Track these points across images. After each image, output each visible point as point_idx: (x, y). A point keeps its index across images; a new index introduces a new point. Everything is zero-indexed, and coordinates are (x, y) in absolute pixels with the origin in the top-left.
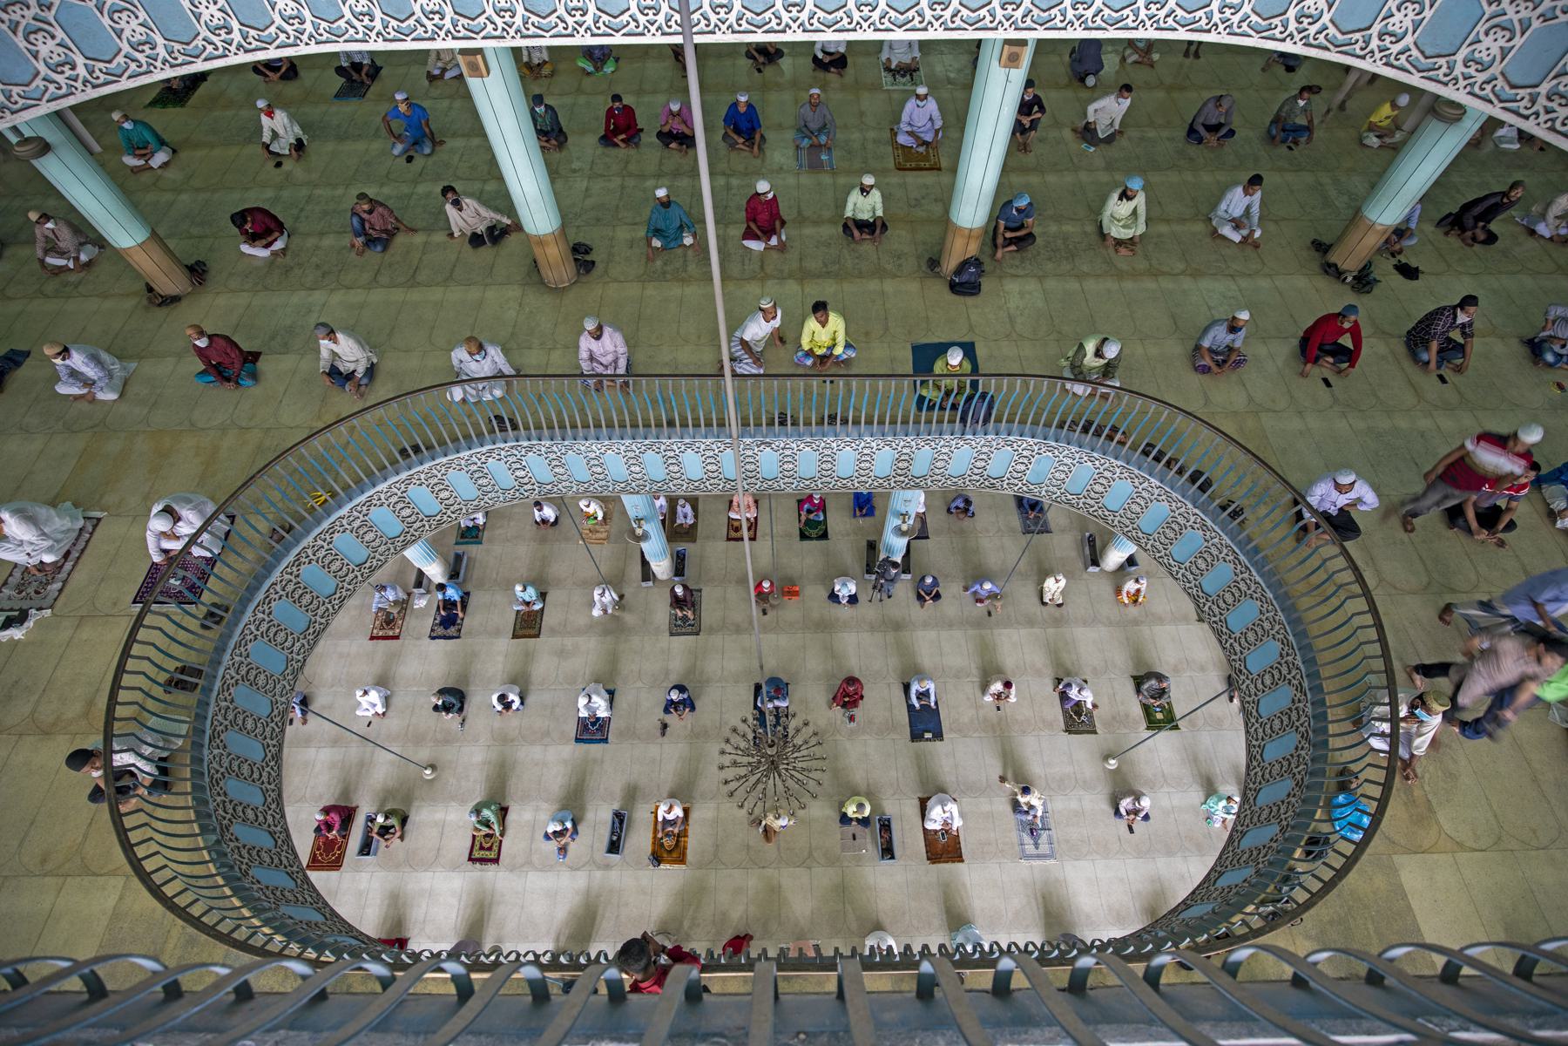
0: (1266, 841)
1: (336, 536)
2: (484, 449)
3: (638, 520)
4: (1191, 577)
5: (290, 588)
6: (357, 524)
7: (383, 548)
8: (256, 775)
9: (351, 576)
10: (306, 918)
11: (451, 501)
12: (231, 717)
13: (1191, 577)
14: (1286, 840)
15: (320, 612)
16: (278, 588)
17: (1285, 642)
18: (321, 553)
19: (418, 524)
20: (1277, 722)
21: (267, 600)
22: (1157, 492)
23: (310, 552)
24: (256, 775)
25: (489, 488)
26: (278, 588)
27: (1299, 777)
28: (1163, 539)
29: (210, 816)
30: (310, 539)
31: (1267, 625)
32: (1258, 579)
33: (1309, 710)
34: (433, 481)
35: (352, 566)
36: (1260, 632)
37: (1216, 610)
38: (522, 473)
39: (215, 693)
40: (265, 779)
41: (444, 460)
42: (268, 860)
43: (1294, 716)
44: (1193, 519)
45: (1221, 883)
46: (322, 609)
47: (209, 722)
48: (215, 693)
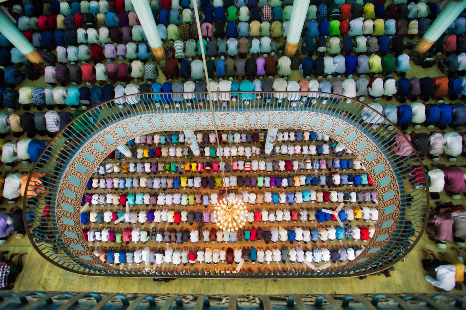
0: (384, 239)
1: (94, 144)
4: (362, 156)
5: (80, 160)
6: (100, 140)
7: (109, 147)
9: (100, 156)
10: (87, 259)
12: (63, 199)
13: (362, 156)
16: (77, 160)
17: (393, 177)
18: (90, 149)
19: (120, 140)
21: (73, 163)
23: (86, 149)
25: (141, 129)
26: (77, 160)
27: (395, 219)
28: (354, 144)
29: (57, 229)
31: (387, 172)
33: (400, 199)
34: (124, 126)
35: (100, 153)
37: (370, 167)
38: (151, 124)
39: (58, 192)
40: (75, 217)
42: (76, 242)
43: (394, 200)
44: (364, 138)
45: (370, 252)
46: (91, 166)
47: (56, 201)
48: (58, 192)
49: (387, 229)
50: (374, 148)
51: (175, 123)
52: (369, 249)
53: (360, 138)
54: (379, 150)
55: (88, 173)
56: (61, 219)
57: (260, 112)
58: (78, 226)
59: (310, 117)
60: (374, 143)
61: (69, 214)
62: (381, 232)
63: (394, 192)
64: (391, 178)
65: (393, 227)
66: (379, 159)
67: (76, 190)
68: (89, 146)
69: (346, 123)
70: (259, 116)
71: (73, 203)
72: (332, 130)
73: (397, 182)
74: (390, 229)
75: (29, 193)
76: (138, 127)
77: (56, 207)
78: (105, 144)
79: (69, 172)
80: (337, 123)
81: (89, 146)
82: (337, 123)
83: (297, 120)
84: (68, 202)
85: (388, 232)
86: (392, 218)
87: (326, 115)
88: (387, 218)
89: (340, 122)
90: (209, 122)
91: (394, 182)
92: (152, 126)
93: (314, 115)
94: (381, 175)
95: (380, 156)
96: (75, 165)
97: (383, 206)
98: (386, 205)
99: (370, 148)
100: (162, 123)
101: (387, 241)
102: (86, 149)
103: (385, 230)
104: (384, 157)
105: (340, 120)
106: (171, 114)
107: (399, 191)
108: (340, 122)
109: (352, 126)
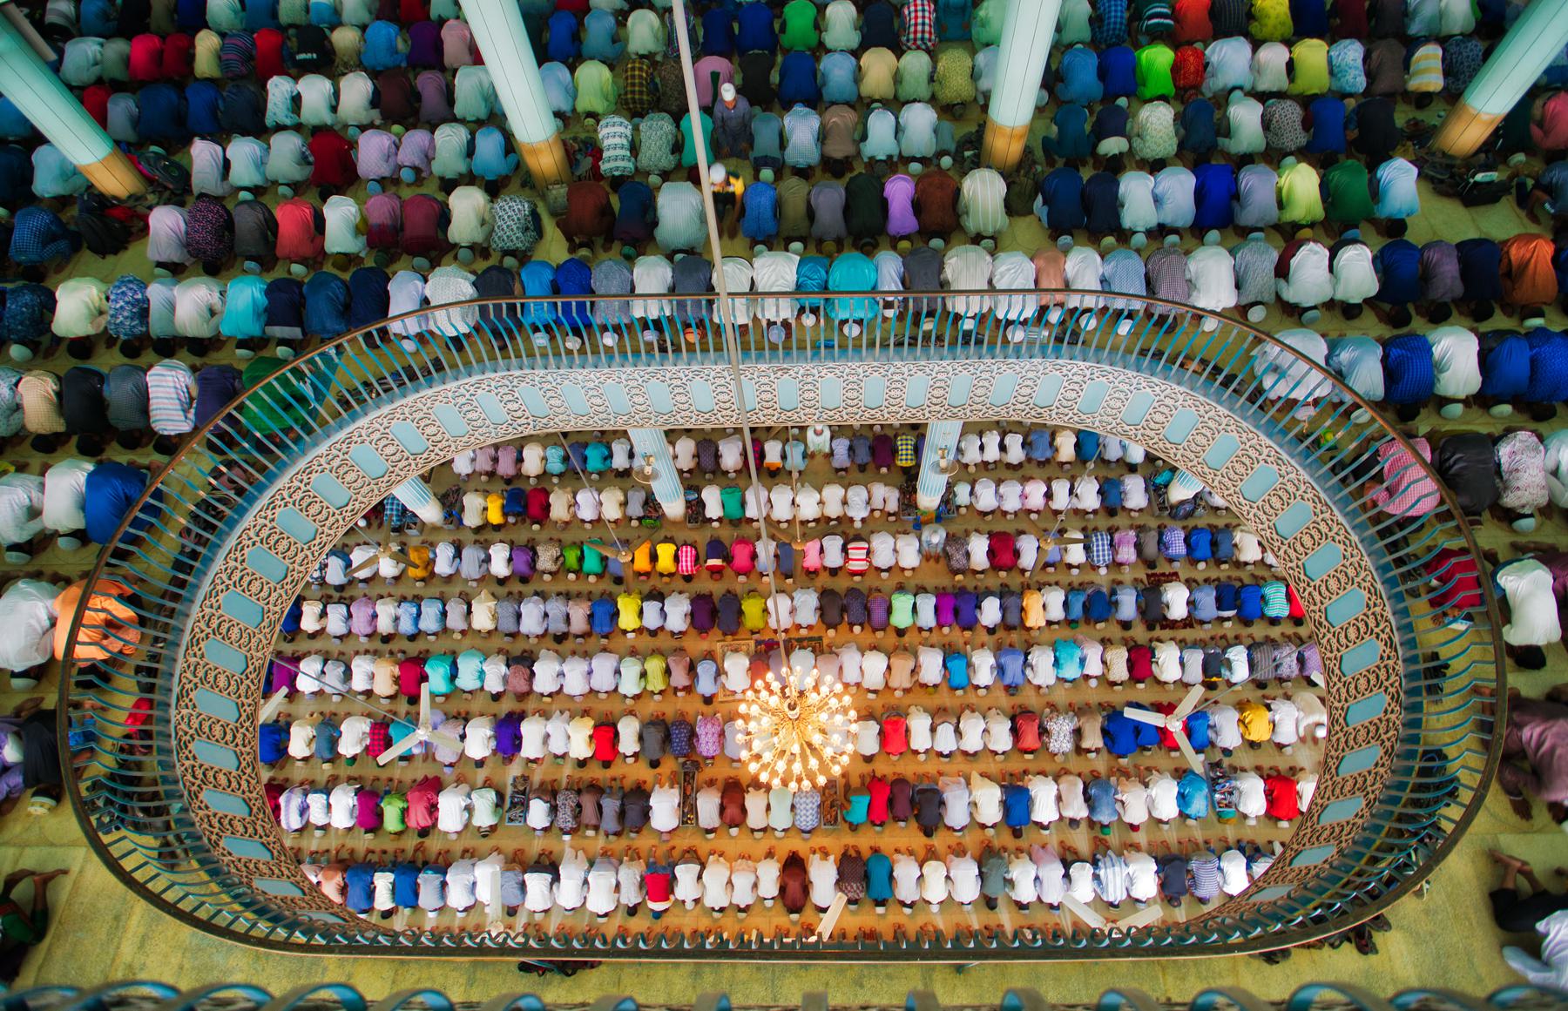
1: (314, 476)
4: (1264, 518)
5: (264, 534)
7: (366, 490)
8: (229, 737)
9: (332, 520)
11: (439, 437)
12: (201, 674)
13: (1264, 518)
14: (1372, 815)
15: (298, 559)
16: (252, 533)
17: (1373, 591)
18: (297, 496)
19: (404, 463)
20: (1362, 681)
21: (240, 547)
22: (1224, 421)
23: (286, 494)
24: (229, 737)
25: (479, 423)
26: (252, 533)
27: (1388, 744)
29: (176, 782)
33: (1400, 668)
35: (332, 509)
37: (1293, 555)
38: (516, 406)
39: (183, 648)
40: (239, 741)
41: (430, 392)
42: (242, 830)
44: (1266, 451)
45: (1299, 863)
46: (301, 556)
47: (176, 679)
49: (1360, 780)
50: (1303, 488)
51: (599, 401)
52: (1298, 853)
53: (1252, 453)
54: (1323, 495)
55: (289, 579)
56: (191, 746)
57: (899, 364)
58: (249, 771)
59: (1075, 379)
61: (217, 728)
63: (1381, 645)
64: (1365, 594)
65: (1382, 770)
67: (245, 640)
68: (296, 484)
69: (1202, 399)
70: (896, 377)
71: (233, 688)
72: (1152, 425)
73: (1387, 608)
74: (1370, 780)
75: (81, 652)
76: (469, 416)
78: (351, 477)
79: (224, 577)
80: (1168, 401)
81: (296, 484)
82: (1168, 401)
83: (1028, 391)
84: (215, 685)
85: (1363, 789)
87: (1131, 373)
88: (1360, 739)
89: (1181, 398)
90: (721, 397)
91: (1378, 609)
92: (519, 414)
93: (1088, 373)
94: (1333, 584)
96: (246, 551)
97: (1344, 695)
99: (1291, 489)
100: (552, 402)
101: (1360, 821)
102: (286, 494)
103: (1351, 783)
104: (1341, 519)
105: (1182, 389)
106: (585, 372)
108: (1181, 398)
109: (1223, 410)
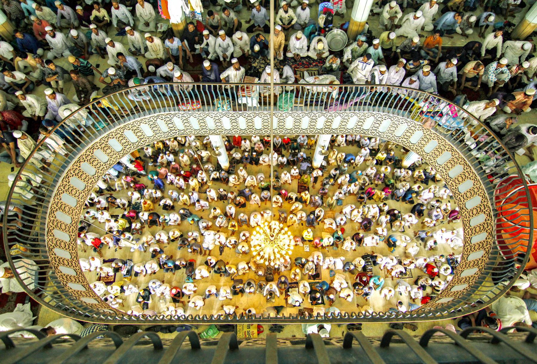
0: (473, 274)
2: (156, 115)
3: (217, 148)
5: (77, 172)
6: (103, 146)
7: (114, 156)
9: (102, 167)
11: (142, 137)
12: (55, 224)
15: (90, 182)
17: (484, 197)
18: (89, 158)
19: (129, 146)
20: (478, 228)
21: (67, 177)
22: (433, 135)
23: (84, 157)
24: (67, 247)
25: (158, 132)
26: (72, 172)
28: (434, 155)
30: (84, 151)
31: (476, 190)
32: (474, 171)
36: (473, 193)
37: (454, 184)
40: (71, 248)
41: (139, 119)
43: (486, 226)
46: (91, 180)
47: (46, 226)
50: (460, 160)
52: (453, 287)
54: (468, 162)
57: (315, 112)
60: (460, 154)
62: (467, 266)
64: (481, 198)
65: (484, 259)
66: (467, 174)
77: (46, 234)
80: (413, 128)
82: (413, 128)
85: (477, 265)
86: (483, 247)
88: (476, 248)
91: (485, 203)
95: (469, 170)
97: (470, 233)
98: (474, 232)
102: (84, 157)
103: (472, 263)
104: (474, 171)
106: (199, 113)
107: (492, 214)
